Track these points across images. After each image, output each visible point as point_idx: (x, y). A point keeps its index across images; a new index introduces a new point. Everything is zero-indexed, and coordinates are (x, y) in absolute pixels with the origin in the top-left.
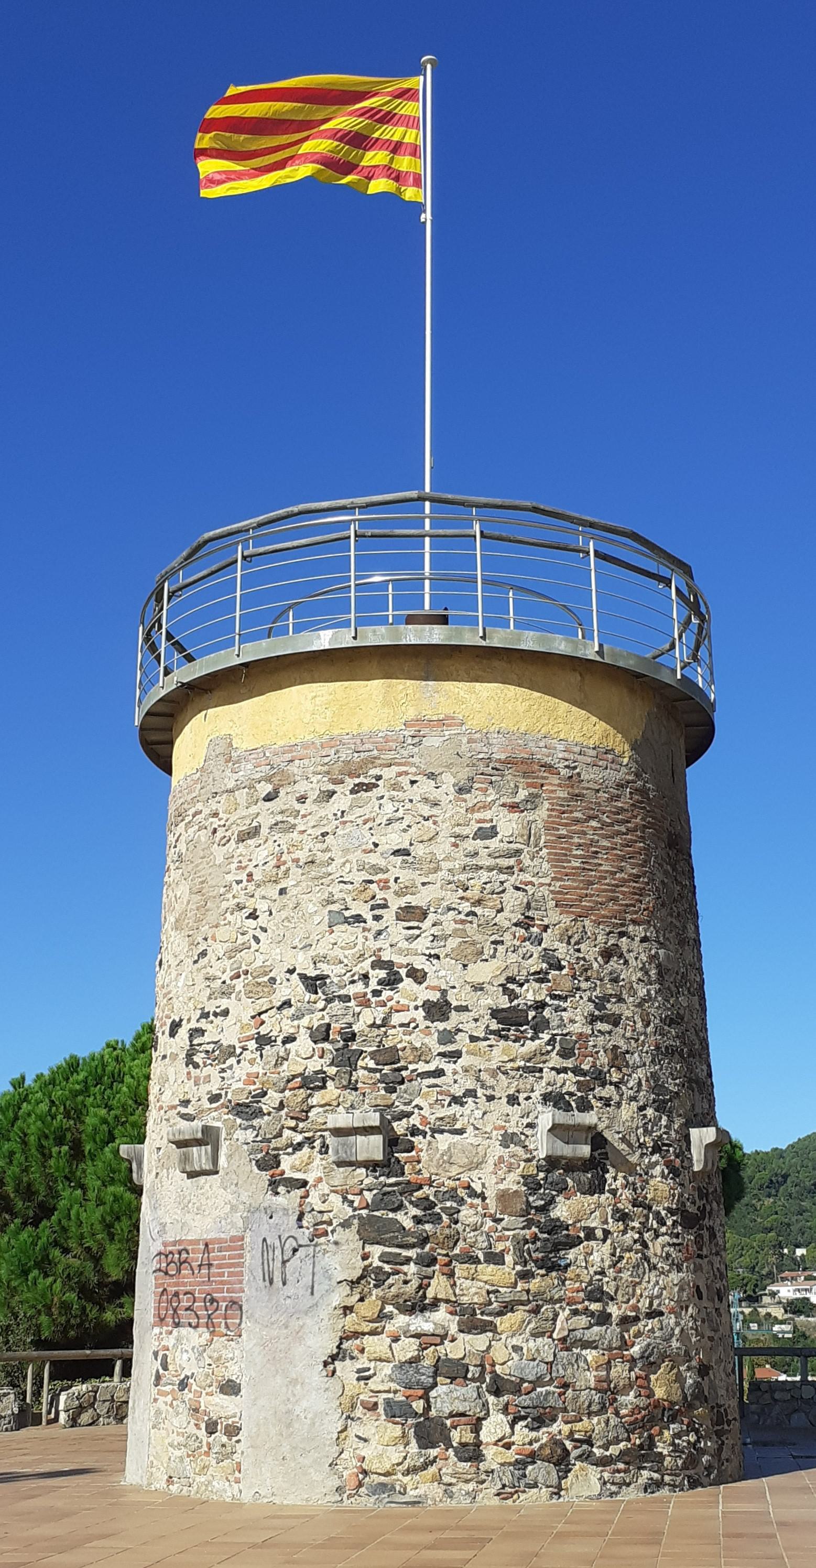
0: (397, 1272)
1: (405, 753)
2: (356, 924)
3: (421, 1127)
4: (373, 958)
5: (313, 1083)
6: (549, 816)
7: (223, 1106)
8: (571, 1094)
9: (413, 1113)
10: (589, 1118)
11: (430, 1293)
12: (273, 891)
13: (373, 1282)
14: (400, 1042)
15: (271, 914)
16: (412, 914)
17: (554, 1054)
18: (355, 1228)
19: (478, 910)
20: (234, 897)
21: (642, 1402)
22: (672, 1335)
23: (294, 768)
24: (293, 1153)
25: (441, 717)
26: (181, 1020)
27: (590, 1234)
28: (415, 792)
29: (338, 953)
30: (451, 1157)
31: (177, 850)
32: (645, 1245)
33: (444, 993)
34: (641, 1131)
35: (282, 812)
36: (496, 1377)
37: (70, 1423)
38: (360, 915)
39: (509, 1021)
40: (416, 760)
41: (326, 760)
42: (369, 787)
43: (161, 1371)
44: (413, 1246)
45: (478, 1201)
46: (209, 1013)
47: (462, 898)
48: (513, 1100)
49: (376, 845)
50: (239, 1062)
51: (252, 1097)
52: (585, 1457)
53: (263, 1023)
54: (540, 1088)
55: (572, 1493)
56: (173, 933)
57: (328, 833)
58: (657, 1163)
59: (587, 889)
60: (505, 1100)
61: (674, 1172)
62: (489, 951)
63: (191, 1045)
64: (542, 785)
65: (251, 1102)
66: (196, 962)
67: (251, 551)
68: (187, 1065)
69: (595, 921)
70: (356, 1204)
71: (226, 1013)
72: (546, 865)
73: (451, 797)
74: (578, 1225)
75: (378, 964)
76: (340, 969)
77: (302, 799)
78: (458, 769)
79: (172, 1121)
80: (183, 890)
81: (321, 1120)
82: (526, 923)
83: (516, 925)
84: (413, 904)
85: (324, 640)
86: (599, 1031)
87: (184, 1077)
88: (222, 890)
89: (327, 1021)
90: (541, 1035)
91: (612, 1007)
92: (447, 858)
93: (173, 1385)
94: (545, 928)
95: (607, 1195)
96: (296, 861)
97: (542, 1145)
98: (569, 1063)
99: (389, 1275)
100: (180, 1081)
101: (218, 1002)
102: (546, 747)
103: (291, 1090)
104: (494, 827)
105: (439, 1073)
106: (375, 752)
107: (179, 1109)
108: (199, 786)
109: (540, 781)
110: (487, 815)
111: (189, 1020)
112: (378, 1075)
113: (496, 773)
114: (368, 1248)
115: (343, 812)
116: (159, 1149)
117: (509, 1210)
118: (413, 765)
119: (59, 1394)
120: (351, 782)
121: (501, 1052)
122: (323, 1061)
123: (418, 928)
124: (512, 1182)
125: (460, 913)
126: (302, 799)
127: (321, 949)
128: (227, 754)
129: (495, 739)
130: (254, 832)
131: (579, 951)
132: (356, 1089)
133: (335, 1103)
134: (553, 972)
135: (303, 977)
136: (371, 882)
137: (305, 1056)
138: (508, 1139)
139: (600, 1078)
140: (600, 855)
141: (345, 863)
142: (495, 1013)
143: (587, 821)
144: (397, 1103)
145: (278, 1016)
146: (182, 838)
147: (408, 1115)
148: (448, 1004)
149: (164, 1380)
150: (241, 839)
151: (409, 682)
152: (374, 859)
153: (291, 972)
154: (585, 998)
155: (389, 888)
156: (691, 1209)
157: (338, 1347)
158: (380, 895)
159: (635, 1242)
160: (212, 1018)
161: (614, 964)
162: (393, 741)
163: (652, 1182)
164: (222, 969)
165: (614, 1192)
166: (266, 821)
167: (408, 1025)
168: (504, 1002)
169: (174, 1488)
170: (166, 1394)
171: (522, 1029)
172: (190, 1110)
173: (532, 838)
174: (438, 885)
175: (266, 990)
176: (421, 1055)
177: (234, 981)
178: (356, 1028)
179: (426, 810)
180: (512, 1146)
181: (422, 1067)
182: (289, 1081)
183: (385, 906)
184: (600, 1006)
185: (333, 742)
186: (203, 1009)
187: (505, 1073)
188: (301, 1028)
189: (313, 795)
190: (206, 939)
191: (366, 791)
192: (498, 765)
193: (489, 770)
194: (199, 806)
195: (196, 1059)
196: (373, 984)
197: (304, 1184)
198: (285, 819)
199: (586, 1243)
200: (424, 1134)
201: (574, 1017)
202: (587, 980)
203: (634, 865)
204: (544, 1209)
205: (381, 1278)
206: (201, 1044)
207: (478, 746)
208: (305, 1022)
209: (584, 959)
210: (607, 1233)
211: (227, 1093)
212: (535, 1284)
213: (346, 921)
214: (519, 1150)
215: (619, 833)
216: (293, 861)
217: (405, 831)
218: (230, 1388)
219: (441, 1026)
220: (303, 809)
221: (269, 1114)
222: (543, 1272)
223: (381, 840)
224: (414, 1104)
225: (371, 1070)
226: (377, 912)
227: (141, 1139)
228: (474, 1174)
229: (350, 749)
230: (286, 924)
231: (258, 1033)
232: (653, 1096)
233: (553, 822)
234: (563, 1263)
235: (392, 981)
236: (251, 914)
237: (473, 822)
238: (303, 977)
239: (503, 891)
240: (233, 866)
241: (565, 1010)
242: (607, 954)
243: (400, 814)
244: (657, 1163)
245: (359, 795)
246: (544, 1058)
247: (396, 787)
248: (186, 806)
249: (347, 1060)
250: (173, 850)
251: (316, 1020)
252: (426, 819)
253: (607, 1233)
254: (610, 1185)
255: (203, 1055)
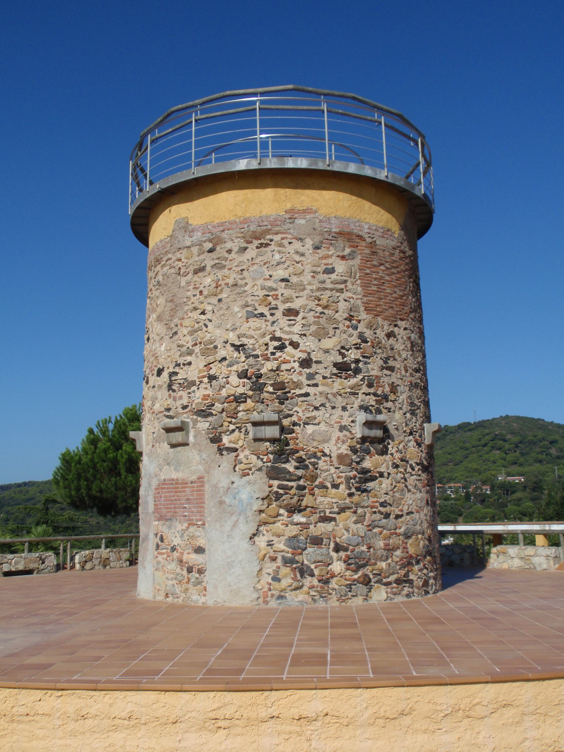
0: (286, 493)
1: (286, 227)
2: (261, 318)
3: (298, 422)
4: (271, 336)
5: (239, 399)
6: (361, 263)
7: (190, 411)
8: (372, 406)
9: (293, 415)
10: (380, 418)
11: (304, 503)
12: (214, 300)
13: (274, 498)
14: (287, 378)
15: (214, 312)
16: (291, 313)
17: (364, 386)
18: (264, 472)
19: (326, 311)
20: (192, 303)
21: (405, 555)
22: (417, 523)
23: (225, 235)
24: (230, 435)
25: (305, 208)
26: (163, 368)
27: (381, 475)
28: (291, 249)
29: (251, 332)
30: (313, 437)
31: (156, 280)
32: (406, 480)
33: (309, 354)
34: (404, 424)
35: (218, 258)
36: (337, 544)
37: (81, 568)
38: (263, 313)
39: (343, 368)
40: (292, 231)
41: (242, 230)
42: (267, 245)
43: (160, 543)
44: (294, 480)
45: (327, 459)
46: (180, 364)
47: (317, 305)
48: (344, 409)
49: (271, 276)
50: (198, 389)
51: (207, 406)
52: (379, 582)
53: (211, 368)
54: (357, 403)
55: (373, 599)
56: (155, 323)
57: (244, 270)
58: (411, 440)
59: (379, 302)
60: (340, 408)
61: (419, 445)
62: (331, 332)
63: (171, 381)
64: (357, 246)
65: (206, 409)
66: (171, 338)
67: (199, 117)
68: (169, 391)
69: (383, 319)
70: (265, 460)
71: (190, 364)
72: (359, 289)
73: (311, 252)
74: (376, 470)
75: (274, 338)
76: (252, 341)
77: (229, 251)
78: (315, 236)
79: (161, 419)
80: (161, 301)
81: (245, 418)
82: (350, 318)
83: (345, 319)
84: (291, 308)
85: (242, 165)
86: (386, 375)
87: (167, 397)
88: (185, 300)
89: (246, 367)
90: (357, 376)
91: (391, 363)
92: (310, 284)
93: (167, 549)
94: (359, 321)
95: (389, 456)
96: (227, 284)
97: (358, 431)
98: (372, 390)
99: (282, 495)
100: (164, 399)
101: (185, 358)
102: (359, 226)
103: (227, 403)
104: (333, 268)
105: (307, 395)
106: (269, 227)
107: (165, 413)
108: (169, 245)
109: (356, 244)
110: (330, 261)
111: (168, 368)
112: (275, 396)
113: (335, 239)
114: (271, 482)
115: (252, 259)
116: (154, 433)
117: (343, 463)
118: (290, 233)
119: (75, 555)
120: (256, 243)
121: (338, 384)
122: (245, 388)
123: (295, 320)
124: (344, 449)
125: (316, 312)
126: (229, 251)
127: (243, 330)
128: (184, 226)
129: (333, 221)
130: (202, 269)
131: (375, 333)
132: (263, 403)
133: (252, 409)
134: (363, 344)
135: (233, 345)
136: (268, 296)
137: (237, 386)
138: (342, 428)
139: (386, 398)
140: (385, 285)
141: (254, 286)
142: (336, 365)
143: (379, 266)
144: (285, 410)
145: (219, 365)
146: (160, 273)
147: (291, 416)
148: (311, 360)
149: (160, 547)
150: (196, 272)
151: (287, 190)
152: (269, 284)
153: (226, 342)
154: (379, 358)
155: (278, 299)
156: (425, 463)
157: (257, 530)
158: (274, 303)
159: (402, 478)
160: (182, 366)
161: (392, 341)
162: (279, 220)
163: (409, 449)
164: (188, 341)
165: (392, 454)
166: (209, 263)
167: (290, 370)
168: (339, 359)
169: (169, 600)
170: (163, 554)
171: (348, 373)
172: (171, 413)
173: (353, 274)
174: (305, 297)
175: (212, 352)
176: (298, 385)
177: (194, 348)
178: (262, 371)
179: (298, 258)
180: (344, 431)
181: (298, 392)
182: (226, 398)
183: (277, 308)
184: (385, 362)
185: (246, 221)
186: (176, 362)
187: (340, 395)
188: (232, 371)
189: (235, 249)
190: (177, 326)
191: (265, 247)
192: (334, 235)
193: (330, 238)
194: (170, 256)
195: (173, 387)
196: (271, 349)
197: (236, 450)
198: (220, 262)
199: (379, 479)
200: (300, 425)
201: (373, 368)
202: (380, 348)
203: (400, 290)
204: (358, 463)
205: (278, 497)
206: (176, 380)
207: (325, 224)
208: (235, 368)
209: (378, 338)
210: (389, 474)
211: (192, 405)
212: (356, 498)
213: (255, 316)
214: (347, 433)
215: (393, 273)
216: (225, 284)
217: (286, 269)
218: (200, 550)
219: (307, 371)
220: (230, 257)
221: (216, 415)
222: (359, 493)
223: (274, 274)
224: (294, 410)
225: (271, 393)
226: (273, 311)
227: (139, 429)
228: (326, 445)
229: (255, 224)
230: (222, 317)
231: (209, 374)
232: (409, 408)
233: (363, 266)
234: (369, 489)
235: (281, 348)
236: (202, 312)
237: (322, 265)
238: (233, 345)
239: (338, 302)
240: (191, 288)
241: (369, 363)
242: (390, 335)
243: (283, 260)
244: (411, 440)
245: (261, 249)
246: (359, 388)
247: (281, 245)
248: (161, 256)
249: (258, 387)
250: (153, 280)
251: (239, 367)
252: (298, 263)
253: (389, 474)
254: (391, 451)
255: (178, 385)
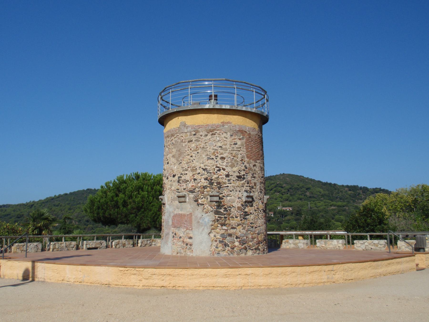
5: (205, 187)
10: (251, 194)
11: (226, 223)
12: (196, 152)
16: (223, 158)
23: (200, 130)
27: (251, 213)
28: (223, 136)
29: (209, 165)
31: (172, 142)
39: (239, 177)
48: (240, 191)
52: (250, 249)
61: (263, 203)
62: (236, 165)
71: (186, 174)
75: (217, 167)
76: (209, 168)
77: (201, 136)
82: (242, 160)
91: (254, 175)
94: (245, 161)
97: (244, 199)
98: (248, 185)
105: (228, 186)
110: (236, 140)
120: (211, 133)
121: (238, 183)
124: (239, 205)
126: (201, 136)
127: (206, 163)
128: (184, 125)
130: (191, 141)
135: (202, 169)
137: (206, 183)
138: (239, 198)
139: (253, 187)
142: (237, 176)
146: (174, 140)
147: (222, 193)
150: (189, 142)
152: (215, 148)
158: (217, 154)
161: (255, 167)
166: (194, 139)
168: (238, 175)
169: (179, 254)
172: (179, 191)
176: (225, 183)
181: (225, 185)
184: (253, 175)
185: (207, 125)
189: (204, 135)
194: (178, 134)
196: (216, 171)
197: (204, 204)
201: (249, 177)
204: (244, 210)
205: (218, 220)
208: (203, 176)
212: (243, 221)
213: (210, 159)
218: (190, 238)
219: (228, 178)
220: (202, 137)
228: (234, 203)
235: (219, 170)
238: (202, 169)
240: (187, 147)
242: (254, 166)
247: (219, 134)
249: (211, 184)
